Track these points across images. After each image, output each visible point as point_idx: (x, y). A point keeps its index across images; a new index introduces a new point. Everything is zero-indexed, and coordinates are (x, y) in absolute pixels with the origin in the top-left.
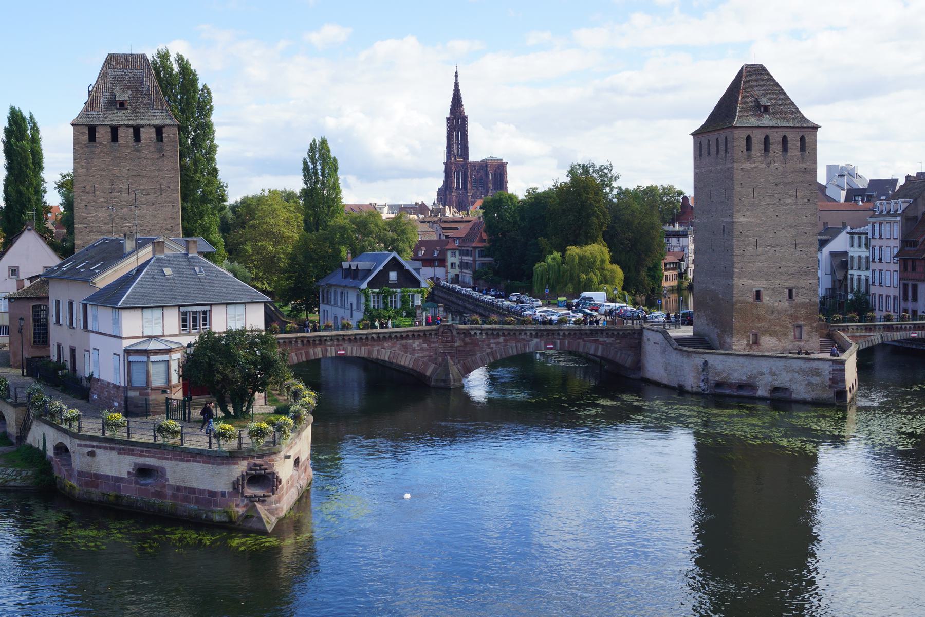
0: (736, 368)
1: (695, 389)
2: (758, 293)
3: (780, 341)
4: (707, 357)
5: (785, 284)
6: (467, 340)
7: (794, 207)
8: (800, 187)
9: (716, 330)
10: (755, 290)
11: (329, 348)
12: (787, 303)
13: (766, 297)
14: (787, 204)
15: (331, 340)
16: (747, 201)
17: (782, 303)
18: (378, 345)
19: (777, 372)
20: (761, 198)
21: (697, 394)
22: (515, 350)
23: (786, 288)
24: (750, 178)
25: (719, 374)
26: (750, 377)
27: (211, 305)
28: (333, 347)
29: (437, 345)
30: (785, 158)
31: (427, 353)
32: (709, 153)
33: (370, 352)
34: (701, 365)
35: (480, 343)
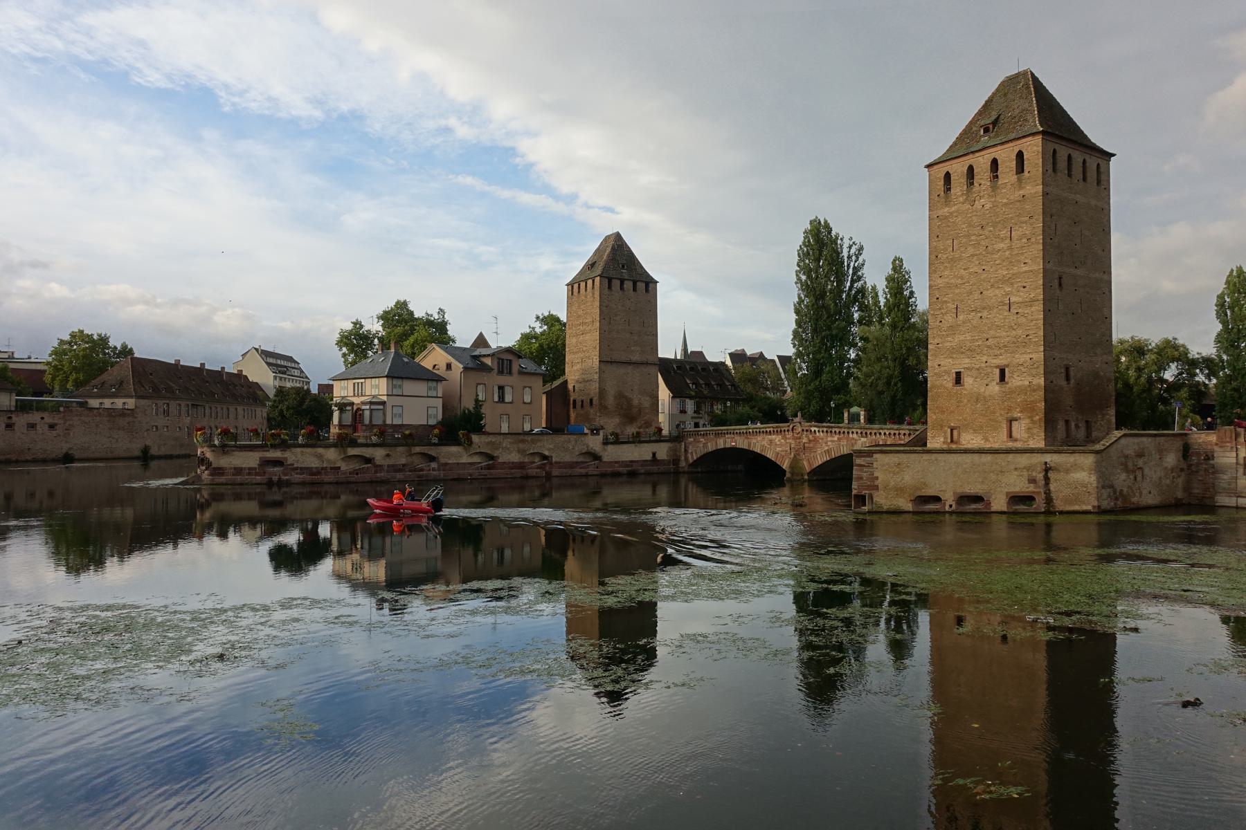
2: (958, 374)
3: (987, 440)
5: (995, 361)
6: (810, 436)
7: (1007, 253)
8: (1016, 224)
10: (954, 371)
12: (997, 388)
13: (968, 381)
14: (999, 250)
16: (945, 256)
17: (990, 387)
20: (962, 249)
22: (845, 448)
23: (997, 367)
24: (949, 226)
27: (365, 378)
29: (790, 441)
30: (994, 188)
33: (749, 444)
35: (820, 441)
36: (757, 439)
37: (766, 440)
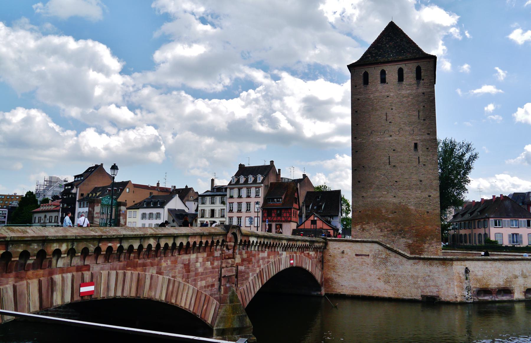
0: (494, 273)
1: (459, 300)
4: (468, 264)
9: (403, 241)
11: (57, 278)
15: (71, 253)
18: (152, 265)
19: (527, 274)
21: (462, 304)
25: (478, 281)
26: (507, 281)
28: (69, 275)
31: (210, 280)
32: (383, 81)
33: (140, 282)
34: (462, 273)
36: (159, 264)
37: (180, 266)
